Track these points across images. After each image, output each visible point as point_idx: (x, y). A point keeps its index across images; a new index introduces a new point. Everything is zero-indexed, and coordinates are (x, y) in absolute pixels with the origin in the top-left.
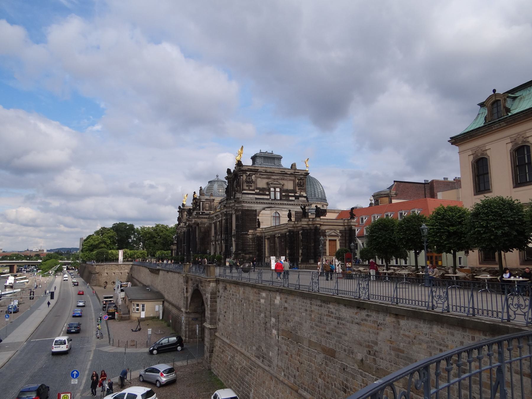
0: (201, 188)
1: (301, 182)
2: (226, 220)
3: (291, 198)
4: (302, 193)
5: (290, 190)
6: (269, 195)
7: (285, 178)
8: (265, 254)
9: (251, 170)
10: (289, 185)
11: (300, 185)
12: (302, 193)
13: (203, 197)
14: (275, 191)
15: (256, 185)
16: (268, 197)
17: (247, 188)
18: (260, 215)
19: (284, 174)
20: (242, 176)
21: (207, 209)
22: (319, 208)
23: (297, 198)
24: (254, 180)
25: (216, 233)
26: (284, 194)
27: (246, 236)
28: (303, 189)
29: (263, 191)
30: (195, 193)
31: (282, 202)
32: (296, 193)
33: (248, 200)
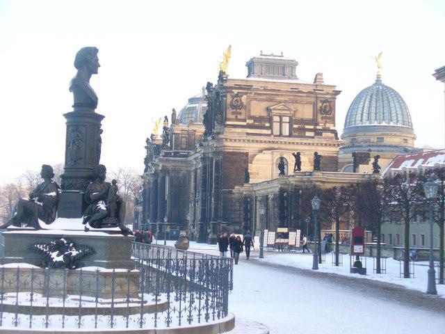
0: (174, 110)
1: (326, 107)
2: (204, 168)
3: (308, 134)
4: (327, 125)
6: (271, 128)
7: (299, 99)
8: (256, 226)
9: (240, 87)
10: (306, 112)
13: (176, 127)
14: (281, 122)
16: (269, 132)
17: (233, 117)
21: (184, 146)
22: (320, 156)
23: (318, 133)
24: (245, 104)
25: (195, 188)
28: (330, 118)
29: (263, 122)
30: (166, 117)
31: (291, 140)
32: (317, 124)
33: (235, 139)
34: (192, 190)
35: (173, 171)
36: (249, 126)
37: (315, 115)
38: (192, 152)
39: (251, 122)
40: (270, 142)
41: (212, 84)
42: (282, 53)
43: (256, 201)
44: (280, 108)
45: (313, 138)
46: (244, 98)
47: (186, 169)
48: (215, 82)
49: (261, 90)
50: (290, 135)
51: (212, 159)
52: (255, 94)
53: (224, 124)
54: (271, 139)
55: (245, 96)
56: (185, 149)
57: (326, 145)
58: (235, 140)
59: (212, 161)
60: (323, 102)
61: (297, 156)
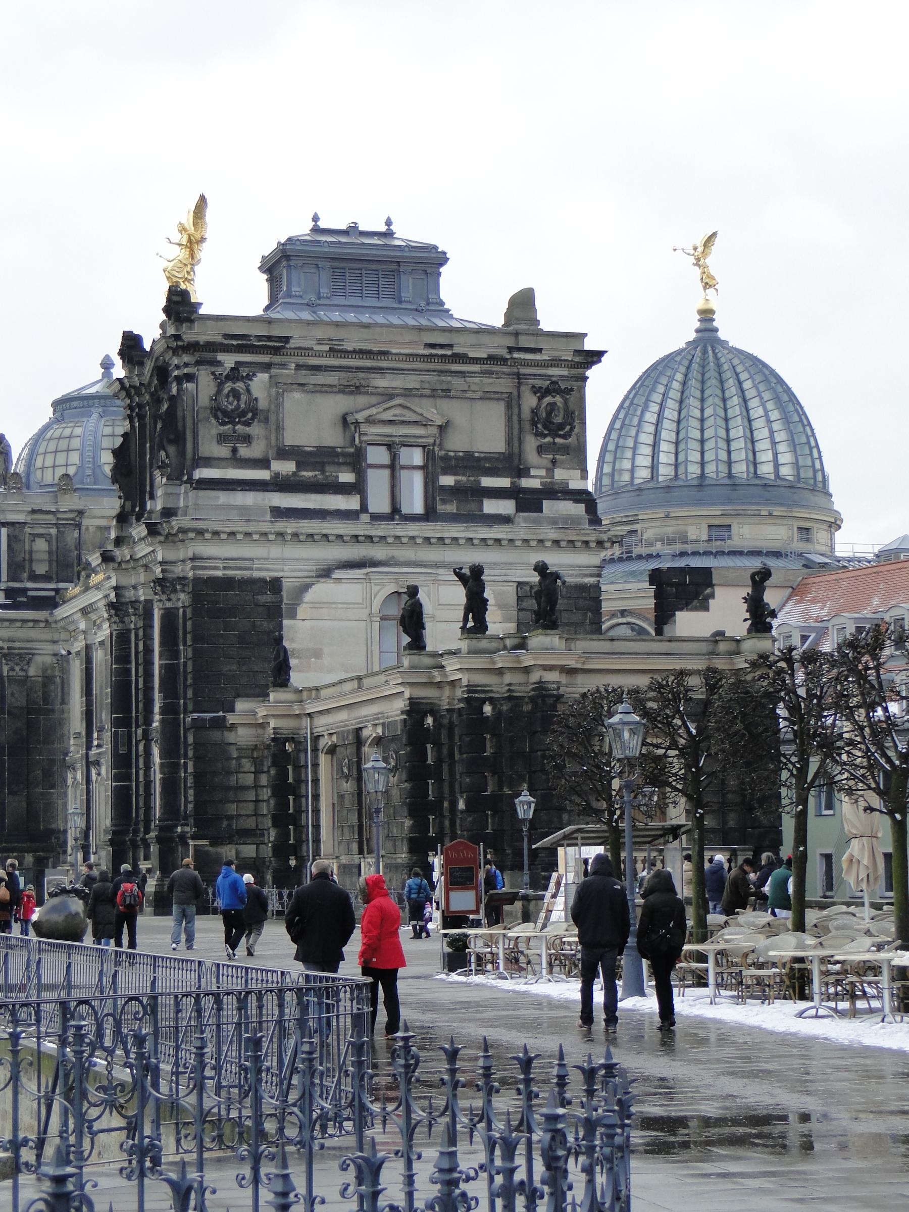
2: (121, 640)
3: (491, 507)
4: (560, 474)
5: (489, 457)
6: (358, 488)
7: (457, 383)
8: (317, 841)
10: (482, 429)
11: (548, 423)
12: (560, 474)
14: (393, 467)
15: (279, 429)
16: (352, 503)
17: (223, 451)
18: (301, 612)
19: (450, 356)
20: (190, 378)
23: (529, 502)
24: (262, 404)
26: (447, 481)
27: (216, 735)
28: (565, 450)
29: (324, 469)
31: (432, 530)
32: (522, 472)
34: (76, 724)
37: (514, 438)
38: (72, 590)
39: (287, 467)
42: (389, 223)
43: (315, 750)
44: (388, 416)
45: (505, 520)
46: (260, 384)
48: (150, 331)
49: (319, 354)
50: (430, 514)
51: (149, 604)
52: (299, 367)
53: (190, 480)
54: (361, 527)
55: (262, 377)
56: (46, 578)
57: (556, 542)
58: (232, 534)
59: (148, 615)
60: (541, 393)
61: (473, 580)
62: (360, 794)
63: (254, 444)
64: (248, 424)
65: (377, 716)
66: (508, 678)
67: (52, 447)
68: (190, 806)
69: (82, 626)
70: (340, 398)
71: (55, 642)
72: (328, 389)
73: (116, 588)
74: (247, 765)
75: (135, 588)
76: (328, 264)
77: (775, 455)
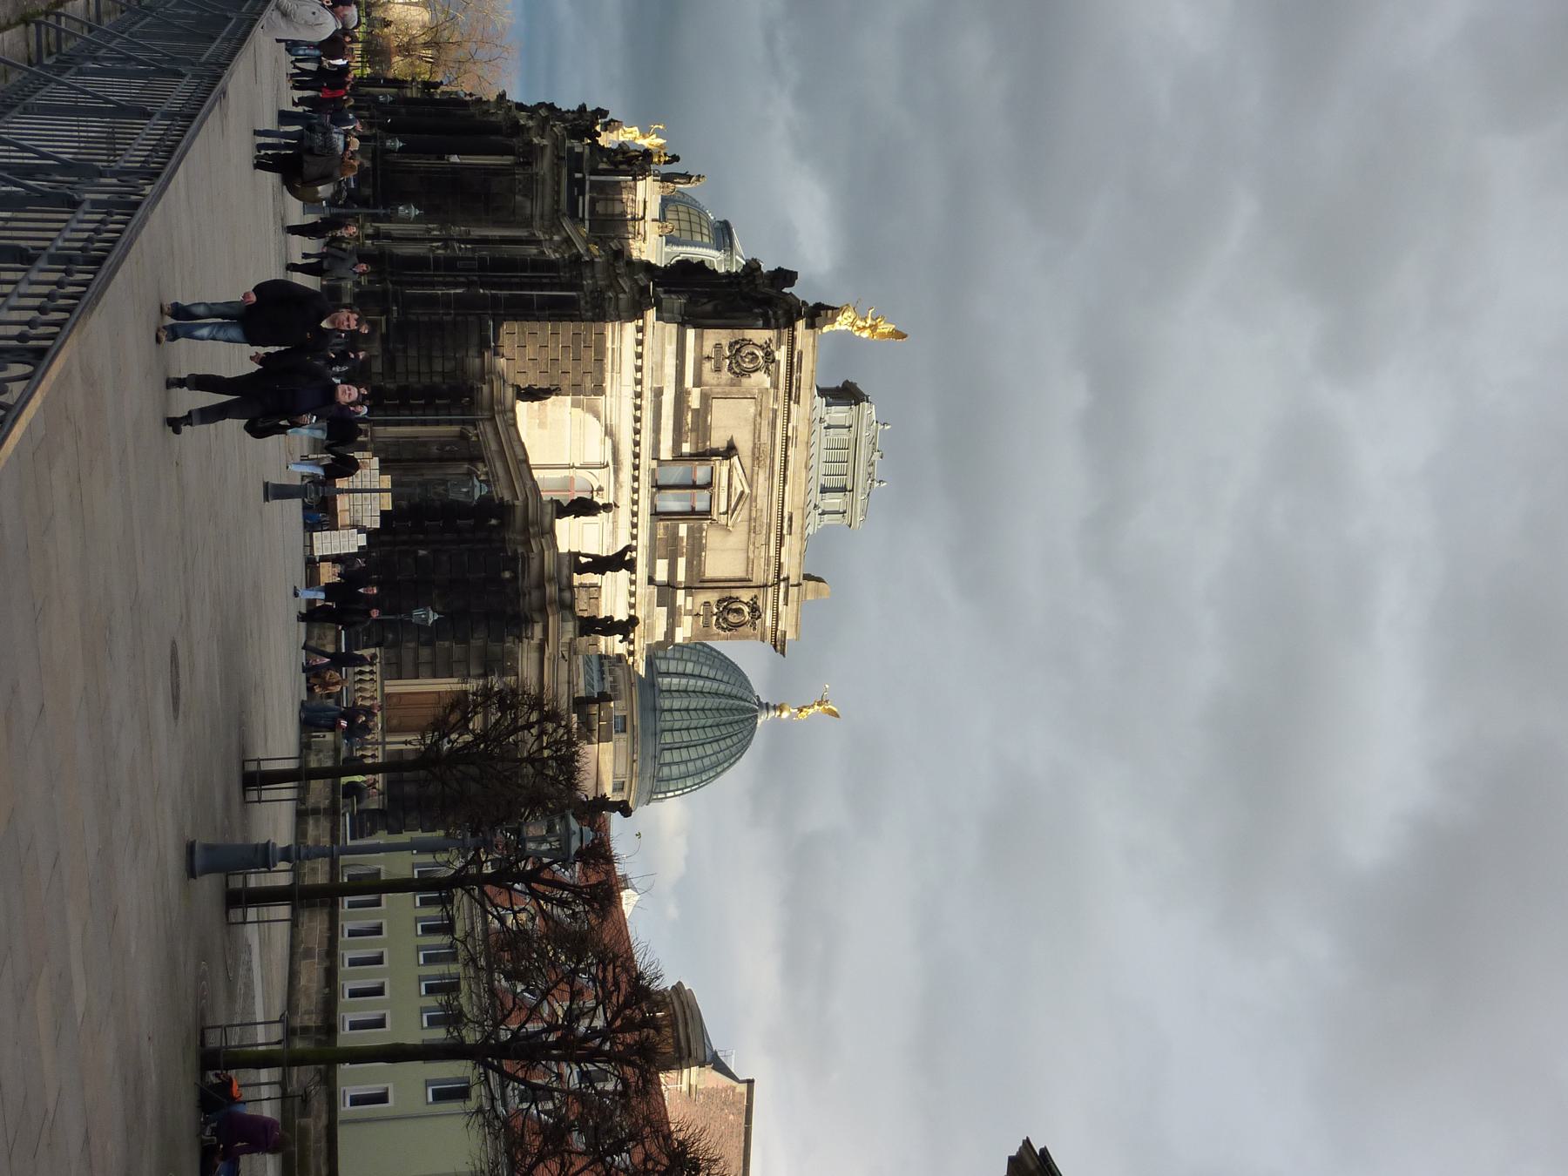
1: (739, 611)
2: (551, 266)
4: (687, 621)
7: (762, 539)
8: (386, 424)
16: (666, 454)
17: (708, 349)
18: (578, 411)
21: (600, 208)
24: (745, 381)
25: (484, 241)
26: (683, 529)
27: (475, 339)
28: (707, 625)
32: (689, 589)
34: (477, 232)
35: (532, 180)
36: (681, 396)
39: (695, 401)
40: (636, 456)
41: (791, 284)
43: (464, 422)
47: (537, 212)
50: (656, 514)
54: (646, 461)
56: (593, 211)
62: (429, 460)
63: (715, 375)
64: (730, 369)
65: (495, 475)
66: (535, 595)
67: (693, 218)
68: (414, 318)
69: (556, 238)
70: (750, 445)
71: (542, 217)
72: (756, 433)
73: (592, 262)
74: (449, 366)
75: (593, 277)
76: (852, 436)
77: (677, 763)
